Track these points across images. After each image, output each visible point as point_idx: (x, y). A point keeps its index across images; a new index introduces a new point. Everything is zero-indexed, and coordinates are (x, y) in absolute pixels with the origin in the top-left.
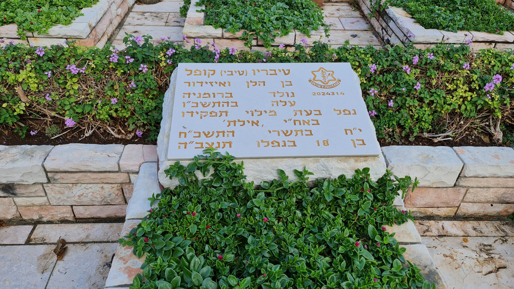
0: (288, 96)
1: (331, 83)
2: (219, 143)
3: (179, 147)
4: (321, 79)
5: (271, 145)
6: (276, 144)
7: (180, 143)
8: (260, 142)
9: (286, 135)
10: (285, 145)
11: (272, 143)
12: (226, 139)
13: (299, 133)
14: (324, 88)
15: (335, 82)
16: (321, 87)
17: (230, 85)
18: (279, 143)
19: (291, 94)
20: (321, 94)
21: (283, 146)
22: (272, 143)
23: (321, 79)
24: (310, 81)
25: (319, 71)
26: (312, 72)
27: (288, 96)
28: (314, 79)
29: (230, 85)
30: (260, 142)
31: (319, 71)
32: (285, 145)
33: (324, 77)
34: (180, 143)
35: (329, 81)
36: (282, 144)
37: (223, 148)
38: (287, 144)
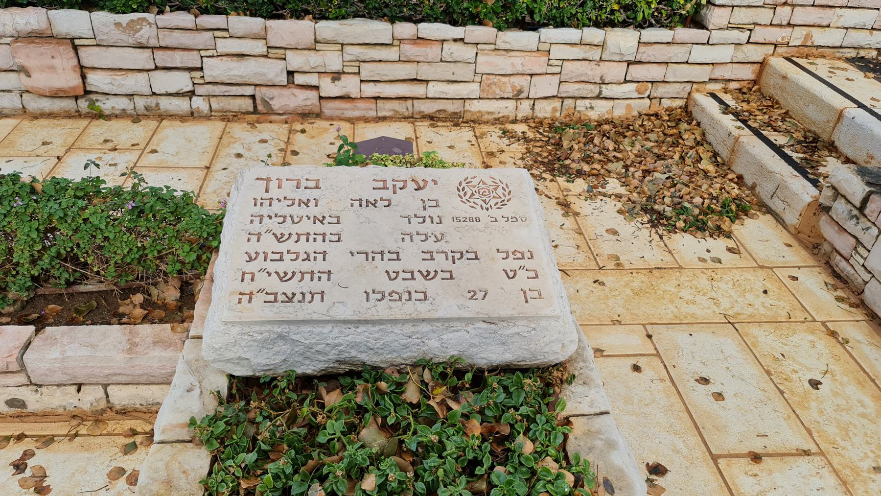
2: (303, 294)
5: (388, 297)
6: (396, 296)
7: (241, 294)
10: (410, 299)
11: (390, 295)
12: (316, 286)
32: (410, 299)
34: (241, 294)
36: (405, 296)
37: (310, 302)
38: (414, 296)
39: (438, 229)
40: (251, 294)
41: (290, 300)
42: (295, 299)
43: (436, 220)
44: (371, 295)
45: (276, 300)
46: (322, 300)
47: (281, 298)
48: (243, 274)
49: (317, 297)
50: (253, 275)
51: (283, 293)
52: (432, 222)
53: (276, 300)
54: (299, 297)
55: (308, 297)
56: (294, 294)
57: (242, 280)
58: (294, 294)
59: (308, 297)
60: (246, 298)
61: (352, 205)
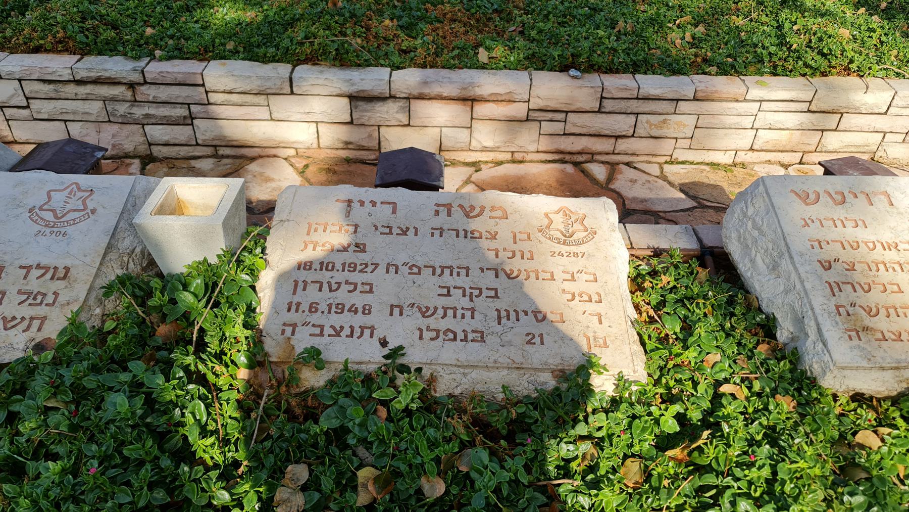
0: (523, 258)
2: (351, 327)
4: (561, 227)
8: (425, 330)
9: (424, 316)
13: (450, 313)
14: (564, 244)
15: (586, 233)
16: (559, 243)
17: (416, 234)
19: (527, 255)
20: (565, 255)
21: (461, 340)
22: (445, 333)
23: (561, 227)
27: (523, 258)
29: (416, 234)
30: (425, 330)
37: (358, 338)
42: (343, 334)
47: (328, 331)
51: (331, 326)
54: (347, 331)
56: (342, 328)
58: (342, 328)
61: (433, 234)
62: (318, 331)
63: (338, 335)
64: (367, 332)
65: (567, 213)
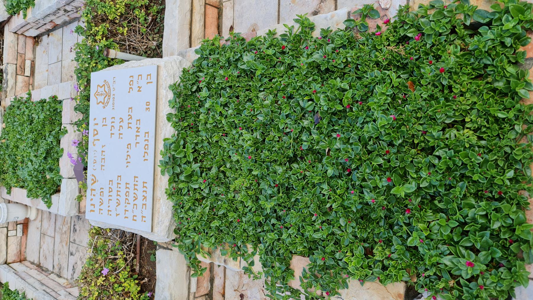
1: (107, 89)
2: (144, 191)
3: (145, 221)
4: (103, 97)
14: (110, 96)
18: (146, 145)
24: (104, 107)
25: (97, 98)
26: (98, 104)
28: (103, 103)
31: (97, 98)
32: (148, 140)
33: (102, 95)
35: (105, 91)
36: (146, 143)
38: (147, 138)
39: (117, 120)
40: (143, 217)
41: (145, 197)
43: (113, 120)
44: (145, 158)
45: (145, 205)
46: (146, 183)
47: (144, 202)
48: (133, 220)
49: (145, 185)
50: (134, 216)
52: (114, 122)
53: (145, 205)
55: (145, 189)
57: (136, 220)
58: (143, 196)
59: (145, 189)
60: (144, 219)
62: (144, 206)
63: (145, 197)
64: (145, 185)
65: (97, 94)
